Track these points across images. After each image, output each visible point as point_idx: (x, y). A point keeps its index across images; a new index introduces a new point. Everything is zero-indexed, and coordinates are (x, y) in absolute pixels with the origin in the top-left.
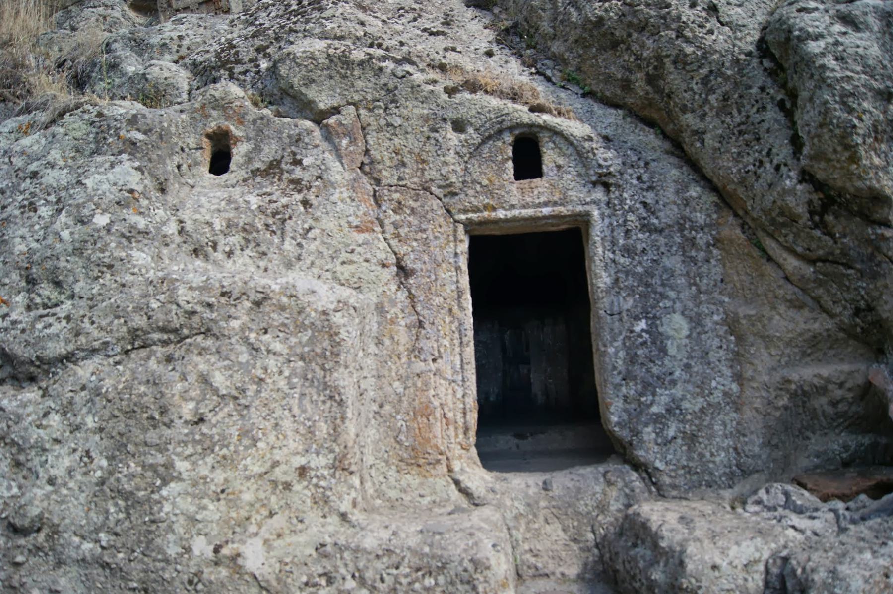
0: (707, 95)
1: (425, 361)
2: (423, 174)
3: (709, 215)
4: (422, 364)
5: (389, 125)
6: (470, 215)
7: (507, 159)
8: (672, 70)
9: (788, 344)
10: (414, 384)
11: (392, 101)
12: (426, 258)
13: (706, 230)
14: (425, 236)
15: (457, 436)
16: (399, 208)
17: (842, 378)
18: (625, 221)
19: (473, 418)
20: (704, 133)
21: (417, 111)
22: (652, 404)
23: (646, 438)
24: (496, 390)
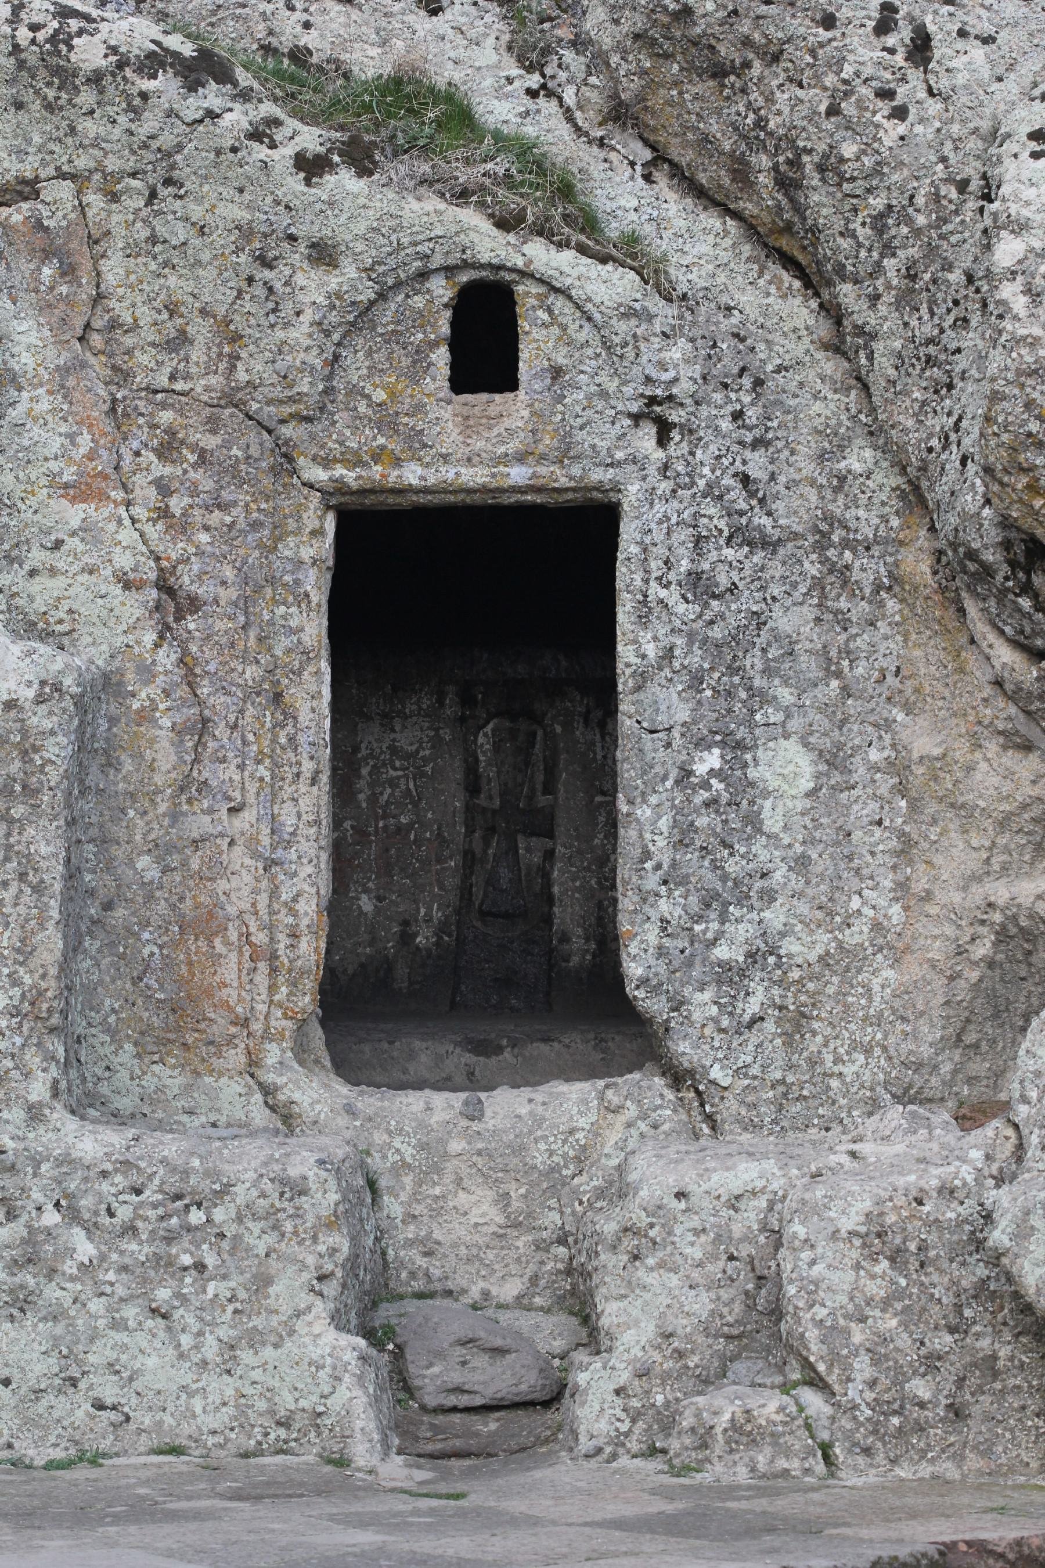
0: (882, 256)
1: (210, 811)
2: (233, 368)
4: (207, 819)
5: (153, 239)
6: (340, 471)
7: (434, 345)
8: (815, 182)
9: (1003, 824)
10: (185, 864)
11: (168, 182)
13: (876, 551)
14: (228, 519)
15: (273, 989)
16: (168, 448)
18: (696, 515)
19: (310, 951)
20: (873, 336)
21: (222, 209)
22: (714, 942)
23: (697, 1016)
24: (437, 915)
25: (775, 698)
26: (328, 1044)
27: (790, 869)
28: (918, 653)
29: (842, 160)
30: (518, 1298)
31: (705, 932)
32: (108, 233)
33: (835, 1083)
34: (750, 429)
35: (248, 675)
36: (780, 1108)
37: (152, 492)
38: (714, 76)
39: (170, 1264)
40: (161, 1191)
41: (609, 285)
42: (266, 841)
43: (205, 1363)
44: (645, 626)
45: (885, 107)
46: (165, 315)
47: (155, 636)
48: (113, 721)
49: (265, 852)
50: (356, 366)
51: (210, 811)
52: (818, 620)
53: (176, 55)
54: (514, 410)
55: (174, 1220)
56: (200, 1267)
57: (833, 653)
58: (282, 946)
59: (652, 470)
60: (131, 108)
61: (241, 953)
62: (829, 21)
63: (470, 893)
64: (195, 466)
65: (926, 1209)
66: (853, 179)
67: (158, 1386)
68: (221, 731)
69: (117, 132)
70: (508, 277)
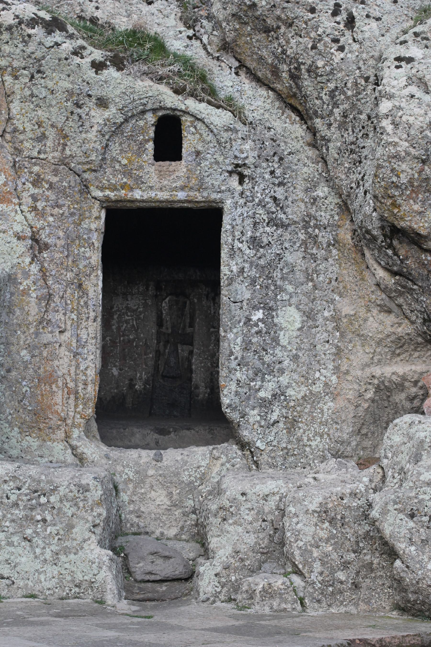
0: (333, 108)
1: (52, 332)
2: (64, 149)
3: (332, 216)
4: (50, 335)
5: (32, 95)
6: (107, 192)
7: (147, 141)
8: (306, 77)
9: (379, 343)
10: (41, 354)
11: (39, 72)
12: (61, 234)
13: (328, 229)
14: (61, 212)
15: (76, 406)
16: (37, 182)
17: (416, 377)
18: (254, 213)
19: (92, 391)
20: (329, 141)
21: (61, 83)
23: (251, 420)
24: (144, 377)
25: (286, 289)
26: (99, 429)
27: (291, 360)
28: (345, 272)
29: (317, 68)
30: (176, 535)
31: (255, 385)
32: (13, 92)
33: (308, 449)
34: (277, 178)
35: (68, 276)
36: (285, 459)
37: (30, 200)
38: (265, 32)
39: (32, 519)
40: (29, 489)
41: (220, 118)
42: (74, 345)
43: (46, 560)
44: (232, 259)
45: (335, 46)
46: (37, 127)
47: (30, 260)
48: (12, 294)
49: (74, 350)
50: (115, 149)
51: (52, 332)
52: (304, 258)
53: (43, 19)
54: (180, 168)
55: (34, 501)
56: (44, 520)
57: (310, 271)
58: (80, 388)
59: (236, 195)
60: (24, 41)
61: (63, 391)
62: (313, 10)
63: (158, 368)
64: (48, 189)
65: (345, 501)
66: (322, 76)
67: (26, 570)
68: (57, 299)
69: (18, 51)
70: (178, 113)
